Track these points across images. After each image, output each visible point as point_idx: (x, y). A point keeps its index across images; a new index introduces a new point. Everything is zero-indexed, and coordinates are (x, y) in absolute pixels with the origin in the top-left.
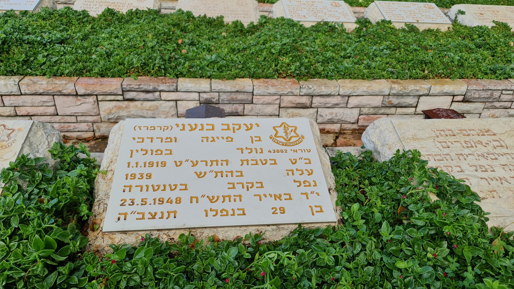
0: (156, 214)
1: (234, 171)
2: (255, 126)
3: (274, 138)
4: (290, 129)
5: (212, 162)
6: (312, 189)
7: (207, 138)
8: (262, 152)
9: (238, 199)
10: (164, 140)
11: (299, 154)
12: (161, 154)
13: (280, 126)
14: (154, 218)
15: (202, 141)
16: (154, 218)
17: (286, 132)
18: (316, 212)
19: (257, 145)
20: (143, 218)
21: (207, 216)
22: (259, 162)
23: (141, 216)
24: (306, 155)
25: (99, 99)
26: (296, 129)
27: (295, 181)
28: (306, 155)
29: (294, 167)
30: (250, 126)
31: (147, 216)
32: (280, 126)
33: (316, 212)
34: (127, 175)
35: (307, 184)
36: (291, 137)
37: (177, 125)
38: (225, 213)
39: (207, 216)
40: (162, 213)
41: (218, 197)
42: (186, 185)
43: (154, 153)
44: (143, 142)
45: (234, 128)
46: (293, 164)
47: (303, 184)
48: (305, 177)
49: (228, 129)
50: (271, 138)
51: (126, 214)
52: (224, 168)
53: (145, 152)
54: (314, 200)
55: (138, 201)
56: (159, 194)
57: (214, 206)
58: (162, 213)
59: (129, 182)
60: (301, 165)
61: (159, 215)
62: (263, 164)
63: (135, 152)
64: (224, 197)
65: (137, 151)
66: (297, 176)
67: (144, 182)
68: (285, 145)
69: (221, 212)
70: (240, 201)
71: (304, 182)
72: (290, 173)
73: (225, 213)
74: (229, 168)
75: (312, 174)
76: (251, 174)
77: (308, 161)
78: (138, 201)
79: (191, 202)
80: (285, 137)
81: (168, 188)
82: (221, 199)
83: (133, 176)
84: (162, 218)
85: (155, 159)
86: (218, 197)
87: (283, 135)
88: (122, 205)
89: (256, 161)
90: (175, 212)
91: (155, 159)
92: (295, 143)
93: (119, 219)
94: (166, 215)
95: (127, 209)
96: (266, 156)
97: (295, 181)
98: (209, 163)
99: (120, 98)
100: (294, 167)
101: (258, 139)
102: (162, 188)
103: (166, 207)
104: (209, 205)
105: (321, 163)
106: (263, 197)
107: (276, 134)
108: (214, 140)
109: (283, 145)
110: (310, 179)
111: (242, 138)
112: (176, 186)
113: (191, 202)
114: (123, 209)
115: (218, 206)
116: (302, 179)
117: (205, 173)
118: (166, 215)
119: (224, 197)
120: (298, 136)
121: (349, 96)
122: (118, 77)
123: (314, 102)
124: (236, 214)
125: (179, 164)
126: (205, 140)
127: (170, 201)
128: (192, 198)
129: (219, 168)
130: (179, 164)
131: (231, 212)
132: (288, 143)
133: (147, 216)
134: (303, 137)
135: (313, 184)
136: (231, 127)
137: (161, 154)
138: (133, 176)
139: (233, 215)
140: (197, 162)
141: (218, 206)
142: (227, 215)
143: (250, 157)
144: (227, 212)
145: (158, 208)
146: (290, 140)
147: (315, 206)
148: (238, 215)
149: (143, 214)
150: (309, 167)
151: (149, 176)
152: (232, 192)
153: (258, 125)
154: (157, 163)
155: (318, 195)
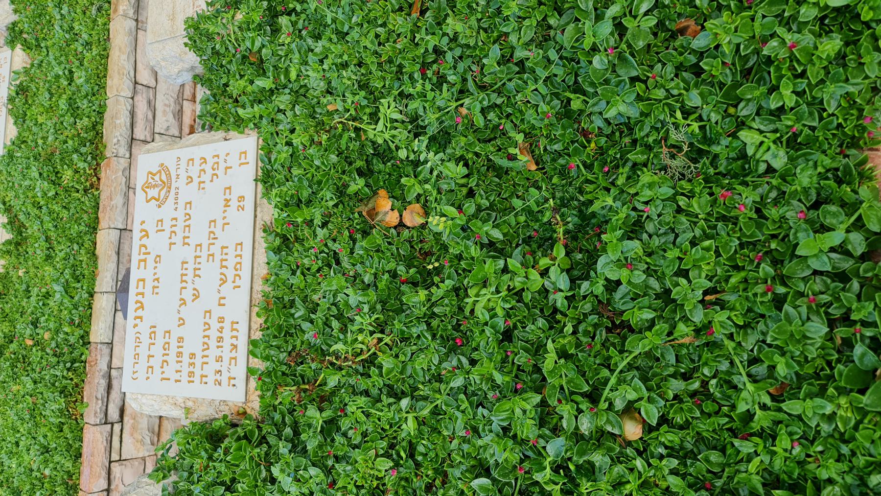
0: (232, 345)
1: (195, 254)
2: (144, 226)
4: (150, 180)
5: (182, 281)
6: (221, 161)
7: (154, 287)
8: (176, 219)
9: (225, 251)
10: (153, 341)
11: (182, 172)
12: (168, 343)
13: (146, 193)
14: (236, 347)
15: (157, 293)
16: (236, 347)
17: (155, 186)
19: (167, 225)
20: (235, 358)
21: (239, 287)
22: (187, 223)
23: (233, 361)
24: (183, 164)
25: (118, 458)
26: (150, 173)
27: (212, 181)
28: (183, 164)
29: (196, 180)
30: (144, 233)
32: (146, 193)
34: (189, 382)
35: (216, 166)
36: (161, 180)
37: (135, 326)
39: (239, 287)
40: (232, 337)
41: (221, 274)
42: (206, 312)
43: (167, 352)
44: (152, 367)
45: (144, 254)
46: (192, 181)
47: (216, 172)
48: (208, 168)
49: (145, 260)
50: (160, 207)
51: (230, 378)
52: (191, 266)
53: (165, 364)
54: (233, 161)
55: (217, 366)
56: (213, 343)
57: (230, 278)
58: (232, 337)
59: (197, 379)
60: (194, 171)
61: (234, 341)
62: (190, 219)
63: (164, 376)
64: (222, 267)
65: (163, 373)
66: (206, 177)
67: (198, 361)
69: (236, 270)
70: (227, 247)
71: (214, 169)
72: (202, 185)
73: (238, 266)
74: (191, 260)
75: (204, 159)
76: (200, 234)
77: (191, 162)
78: (217, 366)
79: (224, 305)
81: (207, 333)
82: (224, 270)
83: (191, 374)
84: (236, 337)
85: (173, 350)
86: (221, 274)
87: (157, 190)
88: (220, 384)
89: (186, 226)
90: (233, 323)
91: (173, 350)
92: (169, 176)
93: (234, 385)
94: (235, 333)
95: (224, 379)
96: (180, 215)
97: (212, 181)
98: (184, 284)
99: (117, 427)
100: (196, 180)
101: (160, 223)
102: (206, 340)
103: (227, 333)
104: (229, 285)
105: (195, 145)
106: (226, 221)
107: (155, 199)
108: (157, 279)
110: (211, 161)
111: (157, 243)
112: (206, 323)
113: (224, 305)
114: (225, 382)
115: (230, 273)
116: (209, 172)
117: (195, 289)
119: (222, 267)
120: (159, 172)
121: (136, 83)
122: (82, 433)
123: (142, 138)
124: (240, 253)
125: (181, 322)
126: (156, 290)
127: (221, 330)
128: (220, 305)
129: (190, 272)
130: (181, 322)
132: (167, 185)
133: (233, 354)
135: (216, 159)
136: (142, 257)
137: (168, 343)
138: (191, 374)
139: (241, 256)
140: (181, 299)
141: (230, 273)
142: (240, 263)
143: (180, 235)
145: (227, 343)
146: (163, 182)
149: (231, 358)
150: (197, 162)
151: (193, 356)
152: (218, 257)
153: (143, 222)
154: (179, 347)
155: (228, 154)
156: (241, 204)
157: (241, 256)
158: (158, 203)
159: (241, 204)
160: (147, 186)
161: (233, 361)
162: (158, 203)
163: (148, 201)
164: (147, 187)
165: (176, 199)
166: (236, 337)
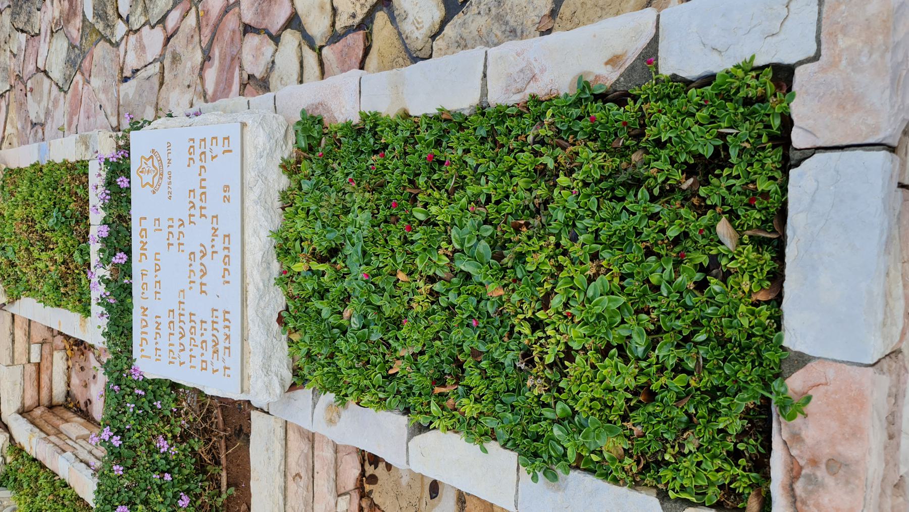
4: (144, 165)
20: (229, 348)
26: (142, 157)
50: (154, 193)
51: (226, 368)
134: (153, 150)
142: (228, 256)
149: (226, 348)
156: (227, 194)
157: (228, 248)
159: (227, 194)
160: (141, 171)
163: (143, 186)
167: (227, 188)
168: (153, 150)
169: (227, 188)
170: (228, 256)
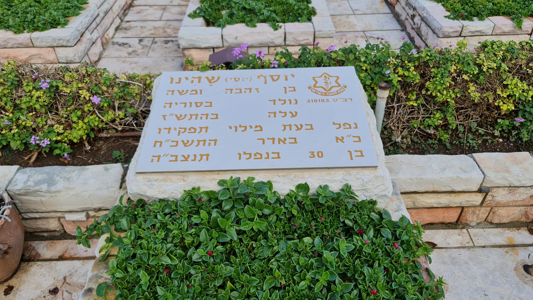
0: (189, 156)
3: (314, 88)
13: (321, 76)
16: (186, 159)
17: (326, 83)
18: (356, 156)
21: (240, 158)
26: (338, 78)
31: (180, 158)
32: (321, 76)
33: (356, 156)
36: (332, 88)
38: (258, 156)
39: (240, 158)
40: (195, 156)
50: (309, 88)
58: (195, 156)
68: (326, 94)
69: (255, 155)
73: (258, 156)
80: (325, 87)
84: (195, 160)
90: (208, 155)
94: (198, 158)
109: (322, 95)
118: (198, 158)
120: (339, 85)
124: (270, 157)
131: (265, 155)
132: (327, 92)
133: (180, 158)
134: (346, 87)
139: (268, 158)
142: (261, 158)
144: (261, 155)
145: (191, 151)
147: (355, 151)
148: (272, 158)
149: (176, 156)
157: (268, 158)
158: (312, 86)
160: (327, 76)
161: (174, 158)
162: (312, 86)
163: (314, 78)
164: (325, 77)
165: (316, 101)
166: (195, 160)
167: (320, 155)
168: (346, 87)
169: (320, 155)
170: (261, 158)
